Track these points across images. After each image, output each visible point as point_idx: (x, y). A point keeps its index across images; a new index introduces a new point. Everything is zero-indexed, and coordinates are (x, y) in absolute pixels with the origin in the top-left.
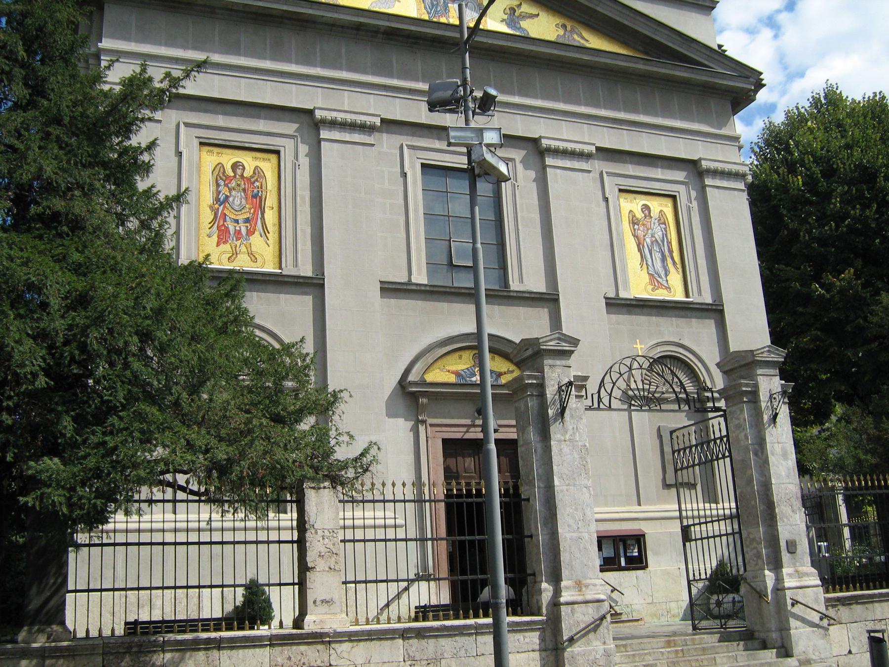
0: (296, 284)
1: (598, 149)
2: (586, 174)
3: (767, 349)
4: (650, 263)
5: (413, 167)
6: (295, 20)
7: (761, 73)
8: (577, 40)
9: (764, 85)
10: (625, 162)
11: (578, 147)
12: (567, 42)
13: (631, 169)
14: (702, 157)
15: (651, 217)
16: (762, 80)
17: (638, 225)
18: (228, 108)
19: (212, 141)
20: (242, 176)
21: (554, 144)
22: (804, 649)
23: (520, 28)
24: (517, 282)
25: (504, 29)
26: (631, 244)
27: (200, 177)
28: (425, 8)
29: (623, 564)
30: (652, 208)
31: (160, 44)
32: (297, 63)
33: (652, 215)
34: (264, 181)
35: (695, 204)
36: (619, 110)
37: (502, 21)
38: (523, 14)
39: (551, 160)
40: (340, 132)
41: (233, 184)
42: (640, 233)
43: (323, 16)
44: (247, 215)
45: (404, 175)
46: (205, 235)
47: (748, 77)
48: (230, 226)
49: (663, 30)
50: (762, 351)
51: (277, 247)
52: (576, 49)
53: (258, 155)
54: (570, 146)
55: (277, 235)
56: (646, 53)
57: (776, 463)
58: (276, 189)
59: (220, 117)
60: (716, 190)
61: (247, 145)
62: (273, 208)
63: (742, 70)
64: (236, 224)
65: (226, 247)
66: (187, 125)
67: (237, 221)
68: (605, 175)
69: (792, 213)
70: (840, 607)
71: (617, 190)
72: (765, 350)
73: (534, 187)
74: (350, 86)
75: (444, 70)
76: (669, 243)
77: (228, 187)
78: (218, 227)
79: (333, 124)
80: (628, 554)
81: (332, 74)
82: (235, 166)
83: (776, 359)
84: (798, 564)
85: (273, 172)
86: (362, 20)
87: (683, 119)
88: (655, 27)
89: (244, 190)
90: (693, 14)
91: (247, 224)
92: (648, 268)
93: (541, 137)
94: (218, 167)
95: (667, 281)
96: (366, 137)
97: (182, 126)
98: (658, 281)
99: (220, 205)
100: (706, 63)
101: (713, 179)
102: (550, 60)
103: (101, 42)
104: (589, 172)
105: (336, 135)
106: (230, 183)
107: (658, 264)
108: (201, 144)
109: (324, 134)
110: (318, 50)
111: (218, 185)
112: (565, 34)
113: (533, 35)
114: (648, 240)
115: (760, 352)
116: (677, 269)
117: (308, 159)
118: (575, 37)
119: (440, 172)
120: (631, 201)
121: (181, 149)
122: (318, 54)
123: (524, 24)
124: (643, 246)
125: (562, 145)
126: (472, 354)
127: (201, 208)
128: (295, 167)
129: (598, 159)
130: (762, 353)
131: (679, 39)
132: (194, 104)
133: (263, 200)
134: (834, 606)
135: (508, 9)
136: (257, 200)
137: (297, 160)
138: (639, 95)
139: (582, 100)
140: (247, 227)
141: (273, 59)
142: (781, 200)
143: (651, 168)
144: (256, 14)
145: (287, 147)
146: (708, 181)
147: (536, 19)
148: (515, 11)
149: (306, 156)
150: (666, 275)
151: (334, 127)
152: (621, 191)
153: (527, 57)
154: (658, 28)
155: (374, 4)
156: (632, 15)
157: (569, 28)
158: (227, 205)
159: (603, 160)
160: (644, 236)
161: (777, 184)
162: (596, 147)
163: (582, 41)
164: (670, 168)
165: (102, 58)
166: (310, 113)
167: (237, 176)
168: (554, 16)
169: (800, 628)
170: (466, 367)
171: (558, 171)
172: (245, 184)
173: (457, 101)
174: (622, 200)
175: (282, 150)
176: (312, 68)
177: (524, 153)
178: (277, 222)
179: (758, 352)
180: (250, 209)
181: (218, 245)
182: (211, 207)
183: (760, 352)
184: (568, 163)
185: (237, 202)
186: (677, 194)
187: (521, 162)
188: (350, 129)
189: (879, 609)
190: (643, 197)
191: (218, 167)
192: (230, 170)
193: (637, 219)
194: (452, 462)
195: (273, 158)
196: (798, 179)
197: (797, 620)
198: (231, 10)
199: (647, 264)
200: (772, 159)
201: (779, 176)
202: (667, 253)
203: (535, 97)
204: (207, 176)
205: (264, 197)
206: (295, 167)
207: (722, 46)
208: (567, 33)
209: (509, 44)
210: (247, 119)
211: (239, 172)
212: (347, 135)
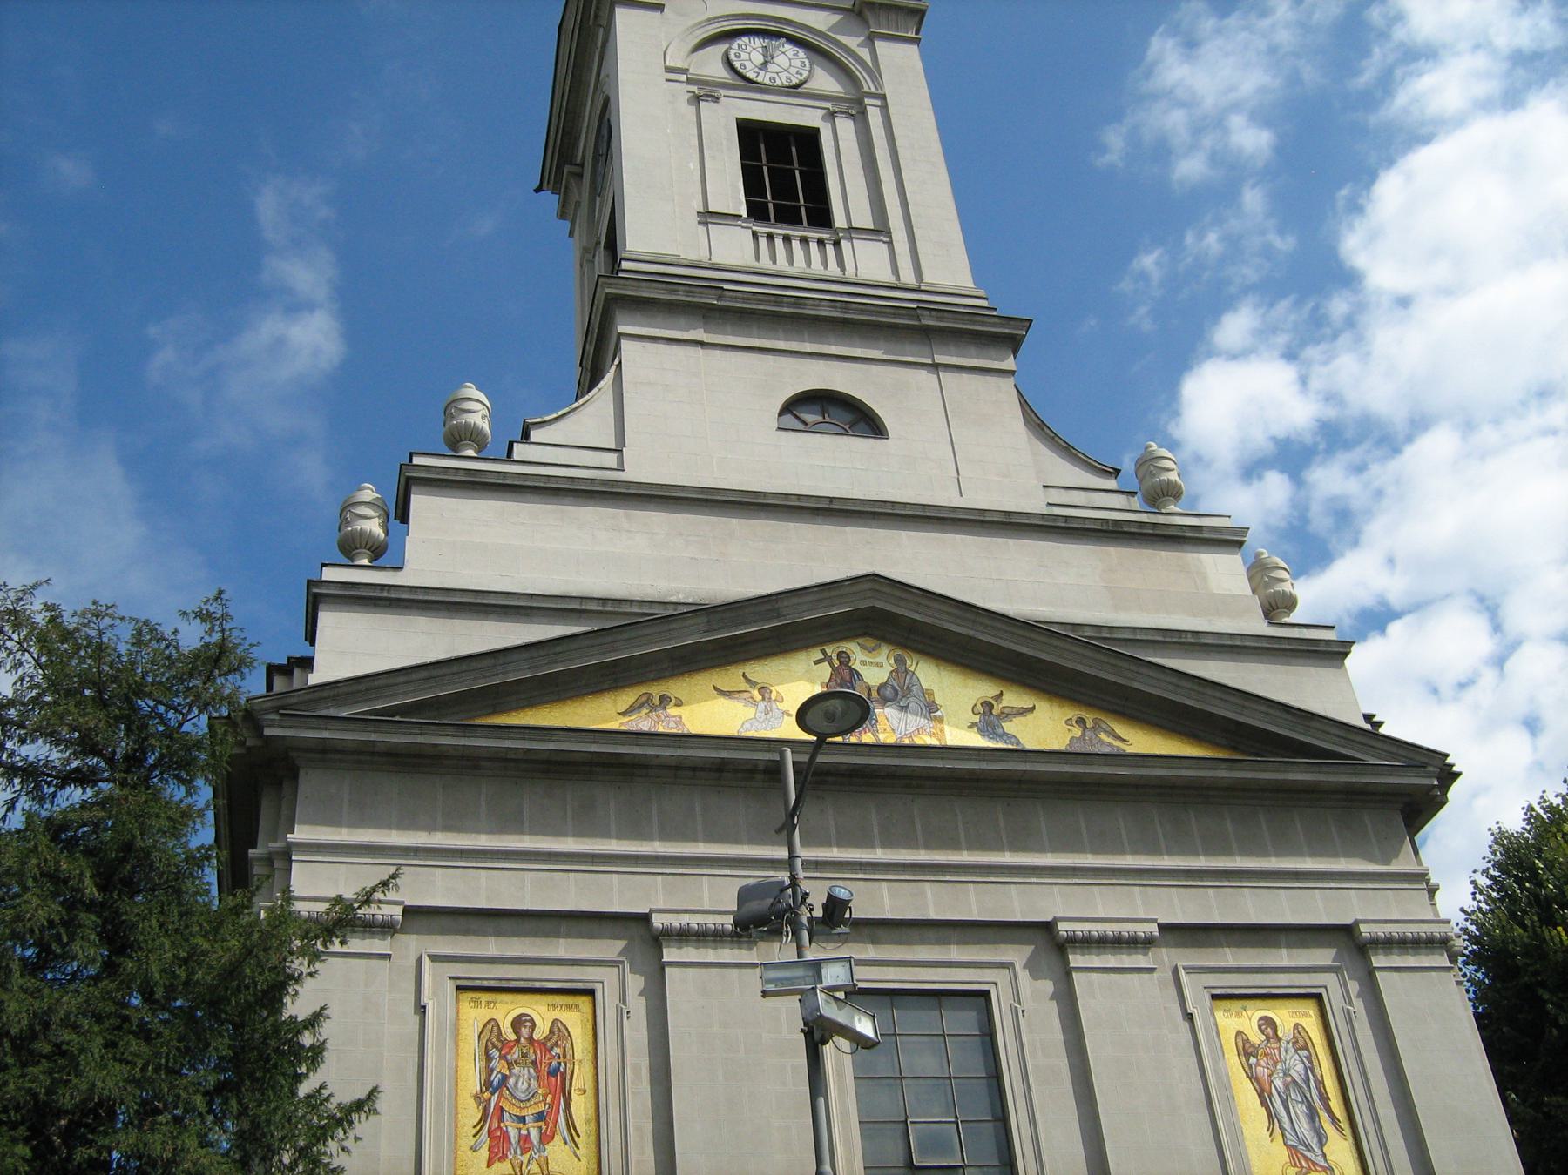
2: (1146, 976)
4: (1287, 1125)
6: (612, 765)
7: (1446, 756)
8: (1106, 742)
9: (1458, 775)
10: (1219, 945)
11: (1126, 929)
12: (1088, 749)
13: (1229, 957)
14: (1360, 918)
15: (1279, 1040)
16: (1452, 766)
17: (1256, 1057)
18: (505, 924)
19: (478, 983)
20: (530, 1039)
21: (1080, 928)
23: (1004, 736)
25: (976, 740)
26: (1246, 1095)
27: (457, 1045)
30: (1278, 1022)
31: (389, 827)
32: (619, 837)
33: (1280, 1035)
34: (569, 1045)
35: (1359, 1006)
36: (1195, 853)
37: (970, 727)
38: (1006, 711)
40: (697, 948)
41: (516, 1054)
42: (1262, 1071)
43: (658, 756)
44: (542, 1107)
46: (466, 1148)
47: (1424, 766)
48: (510, 1129)
49: (1255, 706)
51: (594, 1160)
53: (558, 999)
54: (1110, 929)
55: (593, 1138)
56: (1235, 749)
58: (590, 1056)
59: (491, 940)
60: (1395, 975)
61: (537, 985)
62: (585, 1092)
63: (1411, 755)
64: (521, 1125)
66: (434, 958)
67: (522, 1120)
68: (1182, 973)
69: (1561, 995)
71: (1208, 997)
73: (1053, 1007)
74: (711, 867)
76: (1320, 1083)
77: (507, 1061)
78: (489, 1133)
79: (684, 936)
81: (679, 850)
82: (517, 1023)
85: (584, 1027)
86: (724, 754)
87: (1314, 853)
88: (1240, 701)
89: (534, 1063)
90: (1312, 670)
91: (540, 1124)
92: (1283, 1135)
93: (1056, 920)
94: (489, 1027)
95: (1324, 1155)
96: (743, 951)
97: (426, 961)
98: (1306, 1158)
99: (492, 1094)
100: (1343, 751)
101: (1386, 954)
102: (1060, 783)
103: (293, 832)
104: (1151, 970)
105: (690, 953)
106: (509, 1052)
107: (1304, 1127)
108: (459, 988)
109: (670, 954)
110: (654, 812)
111: (489, 1058)
112: (1083, 734)
113: (1029, 743)
114: (1278, 1083)
116: (1340, 1130)
117: (643, 1000)
118: (1103, 736)
119: (887, 999)
120: (1237, 1014)
121: (425, 1000)
122: (655, 819)
123: (1009, 727)
124: (1270, 1095)
125: (1096, 929)
127: (460, 1101)
128: (623, 1014)
129: (1167, 945)
131: (1289, 717)
132: (445, 921)
133: (568, 1077)
135: (979, 706)
136: (558, 1080)
137: (624, 1002)
138: (1229, 825)
139: (1126, 844)
140: (540, 1128)
141: (579, 833)
142: (1536, 973)
143: (1267, 950)
144: (548, 762)
145: (606, 981)
146: (1378, 961)
147: (1030, 716)
148: (991, 707)
149: (640, 994)
150: (1321, 1144)
151: (687, 941)
152: (1215, 997)
153: (1020, 782)
154: (1246, 704)
155: (747, 725)
156: (1196, 687)
157: (1090, 724)
158: (505, 1092)
159: (1177, 945)
160: (1270, 1076)
161: (1525, 945)
162: (1159, 925)
163: (1116, 743)
164: (1304, 945)
165: (294, 857)
166: (645, 919)
167: (522, 1039)
168: (1061, 706)
171: (1094, 976)
172: (535, 1052)
173: (780, 916)
174: (1219, 1015)
175: (598, 987)
176: (645, 843)
177: (1029, 949)
178: (592, 1112)
180: (545, 1096)
181: (489, 1165)
182: (477, 1097)
184: (1111, 960)
185: (523, 1085)
186: (1322, 991)
187: (1024, 967)
188: (714, 941)
190: (1259, 1003)
191: (489, 1027)
192: (510, 1030)
193: (1253, 1046)
195: (584, 1002)
196: (1559, 933)
199: (1281, 1128)
200: (1513, 899)
201: (1525, 931)
202: (1317, 1103)
203: (1041, 850)
204: (471, 1044)
205: (569, 1072)
206: (623, 1014)
207: (1374, 716)
208: (1088, 733)
209: (984, 765)
210: (537, 940)
211: (525, 1032)
212: (711, 951)
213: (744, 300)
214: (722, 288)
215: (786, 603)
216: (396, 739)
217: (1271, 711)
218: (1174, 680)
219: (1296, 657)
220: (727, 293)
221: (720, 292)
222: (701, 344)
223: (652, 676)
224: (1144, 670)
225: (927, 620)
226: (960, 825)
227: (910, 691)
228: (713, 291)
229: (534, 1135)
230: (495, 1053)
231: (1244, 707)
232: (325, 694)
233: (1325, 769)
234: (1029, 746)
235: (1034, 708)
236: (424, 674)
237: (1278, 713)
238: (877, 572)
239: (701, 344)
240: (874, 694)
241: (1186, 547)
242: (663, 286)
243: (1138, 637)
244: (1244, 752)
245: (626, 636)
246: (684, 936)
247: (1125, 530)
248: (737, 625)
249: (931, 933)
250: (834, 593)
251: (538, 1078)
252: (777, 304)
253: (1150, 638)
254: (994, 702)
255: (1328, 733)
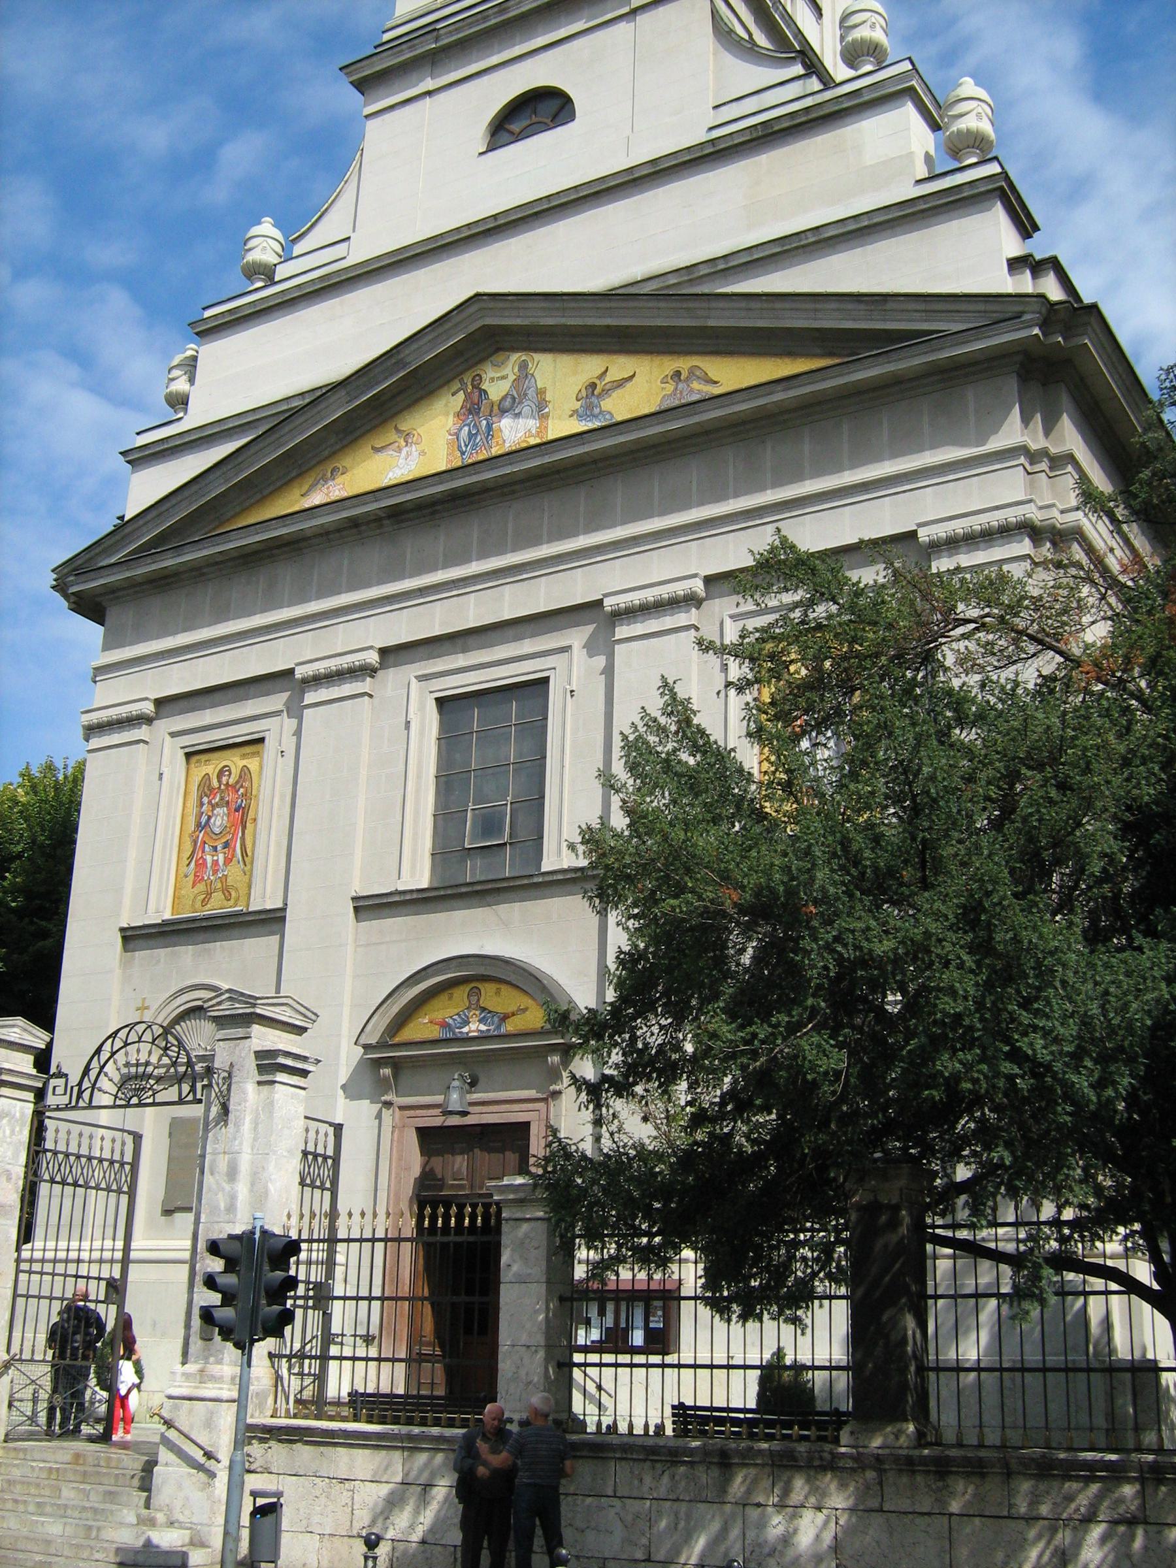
0: (263, 922)
1: (709, 580)
3: (227, 995)
5: (422, 708)
8: (699, 389)
18: (217, 696)
20: (227, 784)
22: (167, 1501)
24: (554, 858)
28: (459, 447)
29: (638, 1338)
37: (571, 416)
38: (607, 387)
39: (625, 627)
45: (408, 723)
49: (827, 306)
50: (219, 999)
52: (654, 419)
56: (831, 354)
57: (214, 1187)
61: (231, 741)
65: (201, 887)
70: (272, 1443)
72: (224, 997)
74: (346, 614)
75: (475, 536)
79: (317, 680)
80: (652, 1325)
82: (220, 775)
83: (241, 1011)
84: (212, 1359)
96: (359, 683)
108: (188, 756)
112: (676, 389)
115: (214, 1002)
118: (696, 385)
126: (468, 989)
130: (219, 1003)
131: (862, 306)
132: (183, 704)
134: (262, 1440)
135: (584, 390)
147: (629, 385)
154: (818, 306)
156: (765, 305)
169: (172, 1466)
170: (456, 1011)
179: (211, 1003)
183: (214, 1002)
184: (653, 625)
189: (346, 1459)
194: (437, 1162)
197: (171, 1451)
198: (217, 563)
209: (547, 459)
211: (224, 779)
213: (457, 30)
214: (435, 30)
215: (407, 352)
216: (140, 571)
217: (842, 306)
218: (743, 304)
219: (939, 214)
220: (442, 32)
221: (435, 34)
222: (429, 93)
223: (326, 453)
224: (714, 305)
225: (526, 322)
226: (546, 518)
227: (526, 395)
228: (428, 37)
229: (221, 858)
230: (205, 800)
231: (816, 310)
232: (97, 551)
233: (894, 356)
234: (619, 418)
235: (634, 375)
236: (154, 513)
237: (850, 306)
238: (482, 290)
239: (429, 93)
240: (496, 408)
241: (848, 120)
242: (389, 52)
243: (756, 257)
244: (840, 356)
245: (287, 429)
246: (317, 680)
247: (776, 128)
248: (371, 388)
249: (510, 632)
250: (447, 326)
251: (229, 815)
252: (486, 19)
253: (767, 253)
254: (598, 382)
255: (907, 311)
